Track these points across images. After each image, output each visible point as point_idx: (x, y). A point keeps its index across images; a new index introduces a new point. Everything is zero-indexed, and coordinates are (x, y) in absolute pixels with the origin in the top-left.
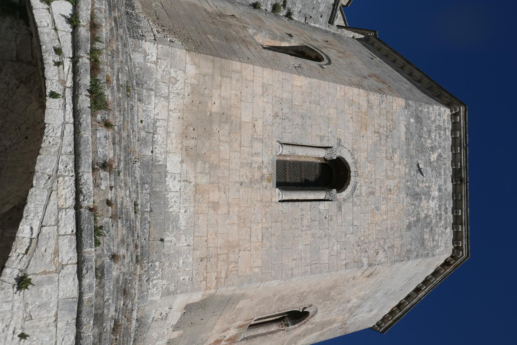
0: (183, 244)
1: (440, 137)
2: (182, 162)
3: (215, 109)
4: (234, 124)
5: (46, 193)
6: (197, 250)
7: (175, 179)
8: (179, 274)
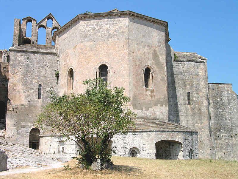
1: (90, 25)
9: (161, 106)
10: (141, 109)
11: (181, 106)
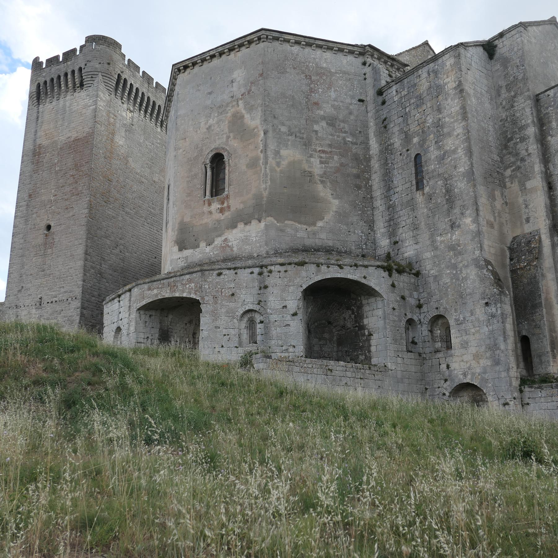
9: (246, 224)
10: (198, 246)
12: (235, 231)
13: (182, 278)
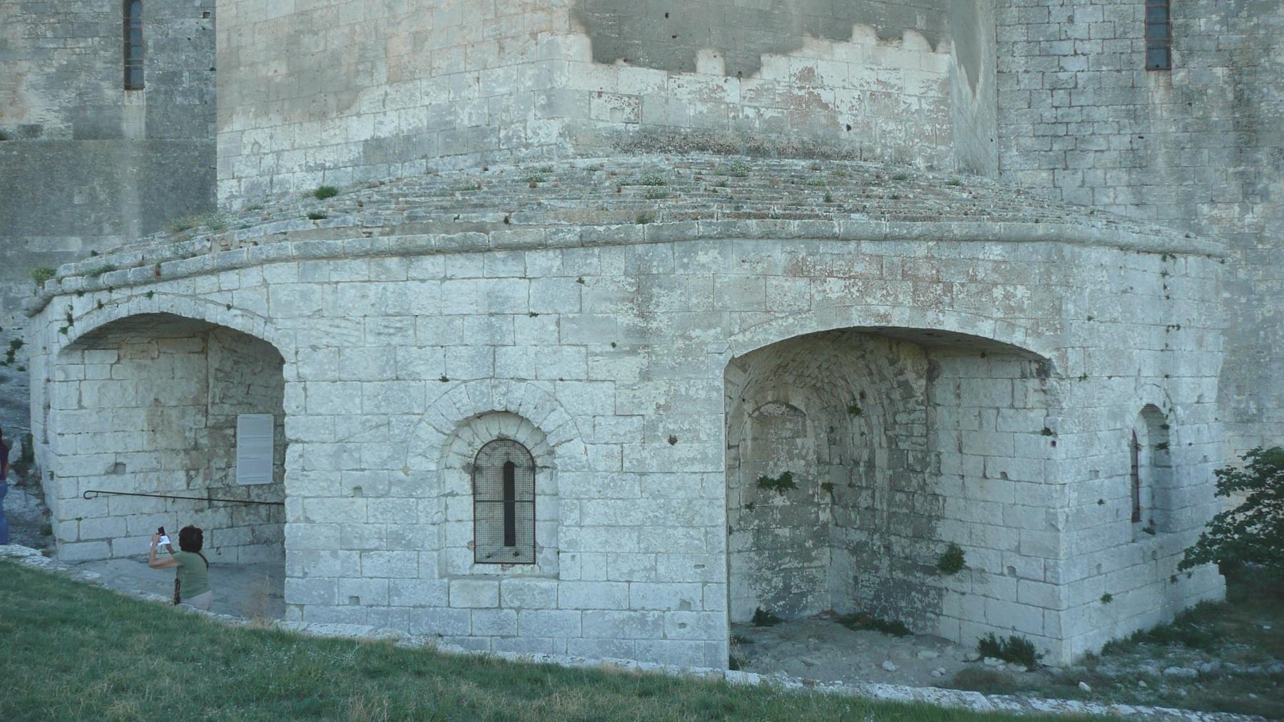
0: (474, 93)
2: (359, 115)
3: (283, 70)
4: (301, 27)
5: (209, 305)
6: (486, 61)
7: (381, 123)
8: (522, 90)
9: (884, 37)
10: (689, 66)
11: (1090, 79)
12: (841, 50)
13: (966, 250)
